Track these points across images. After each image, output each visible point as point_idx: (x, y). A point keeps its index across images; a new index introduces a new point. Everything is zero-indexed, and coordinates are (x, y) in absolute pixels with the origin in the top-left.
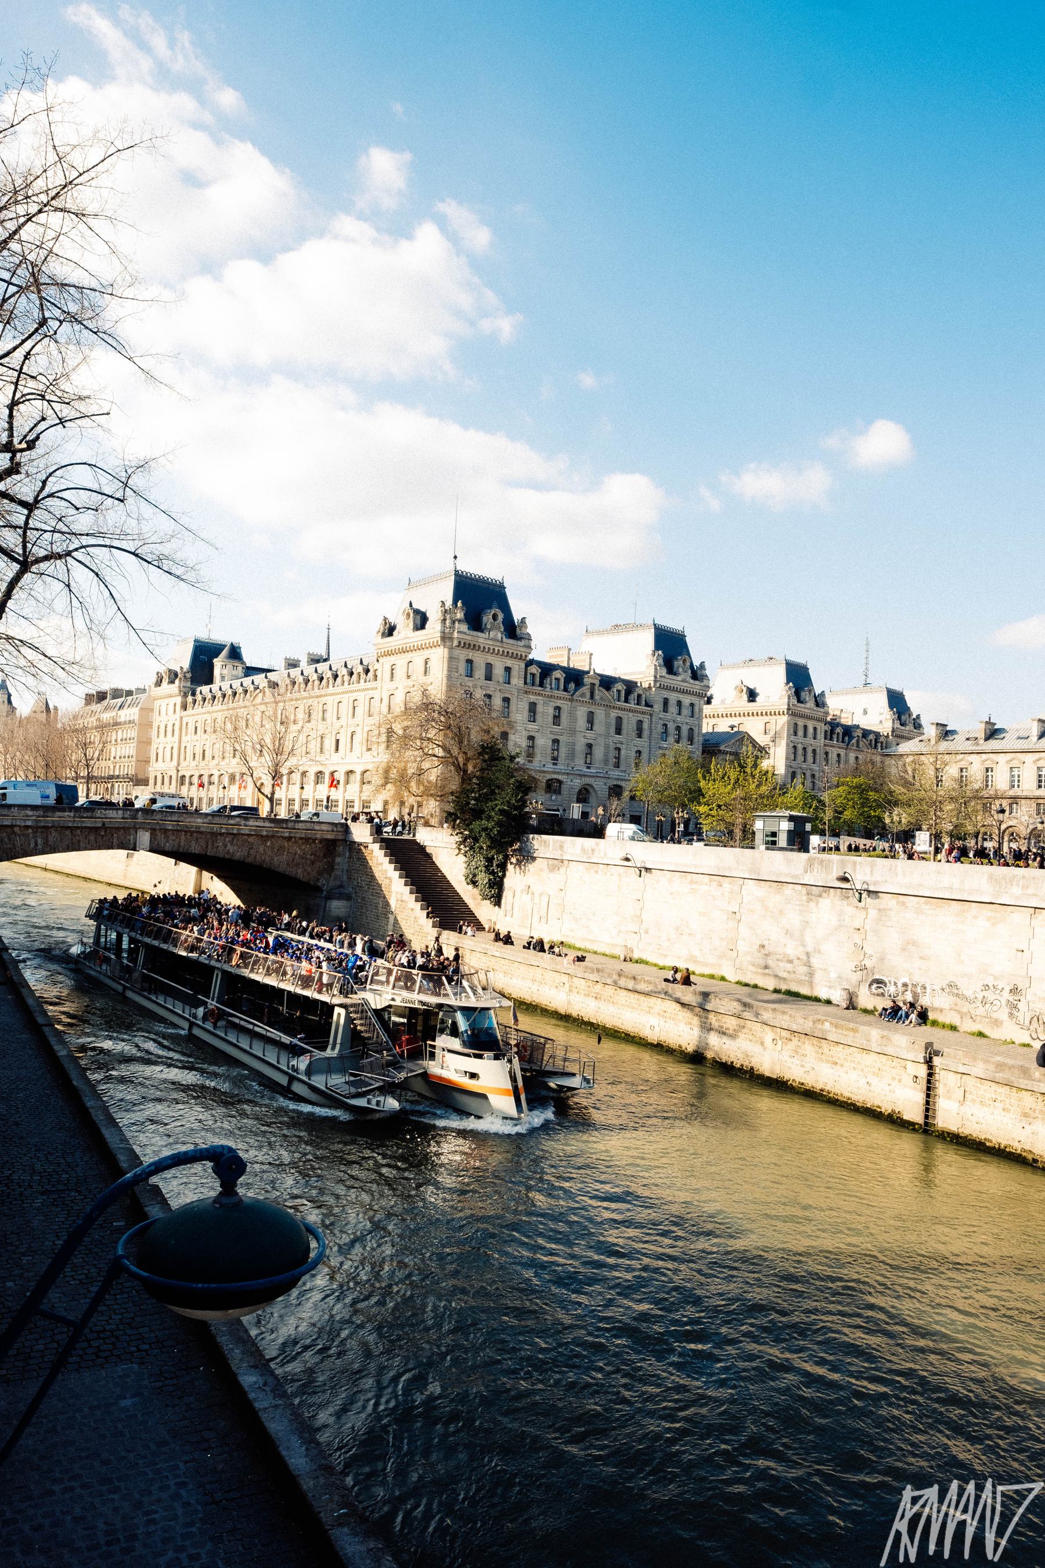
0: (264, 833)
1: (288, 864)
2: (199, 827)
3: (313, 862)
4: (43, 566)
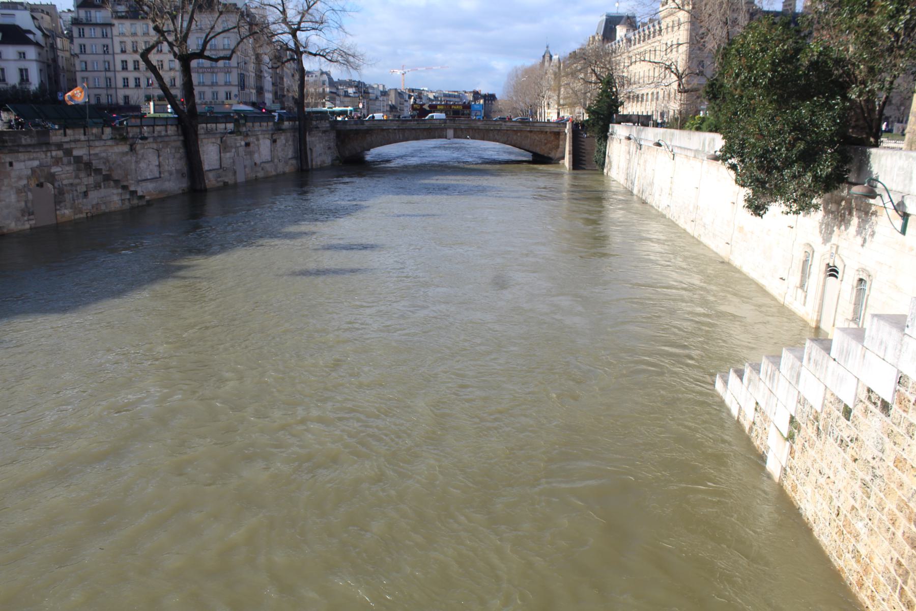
0: (515, 129)
3: (546, 144)
4: (351, 14)
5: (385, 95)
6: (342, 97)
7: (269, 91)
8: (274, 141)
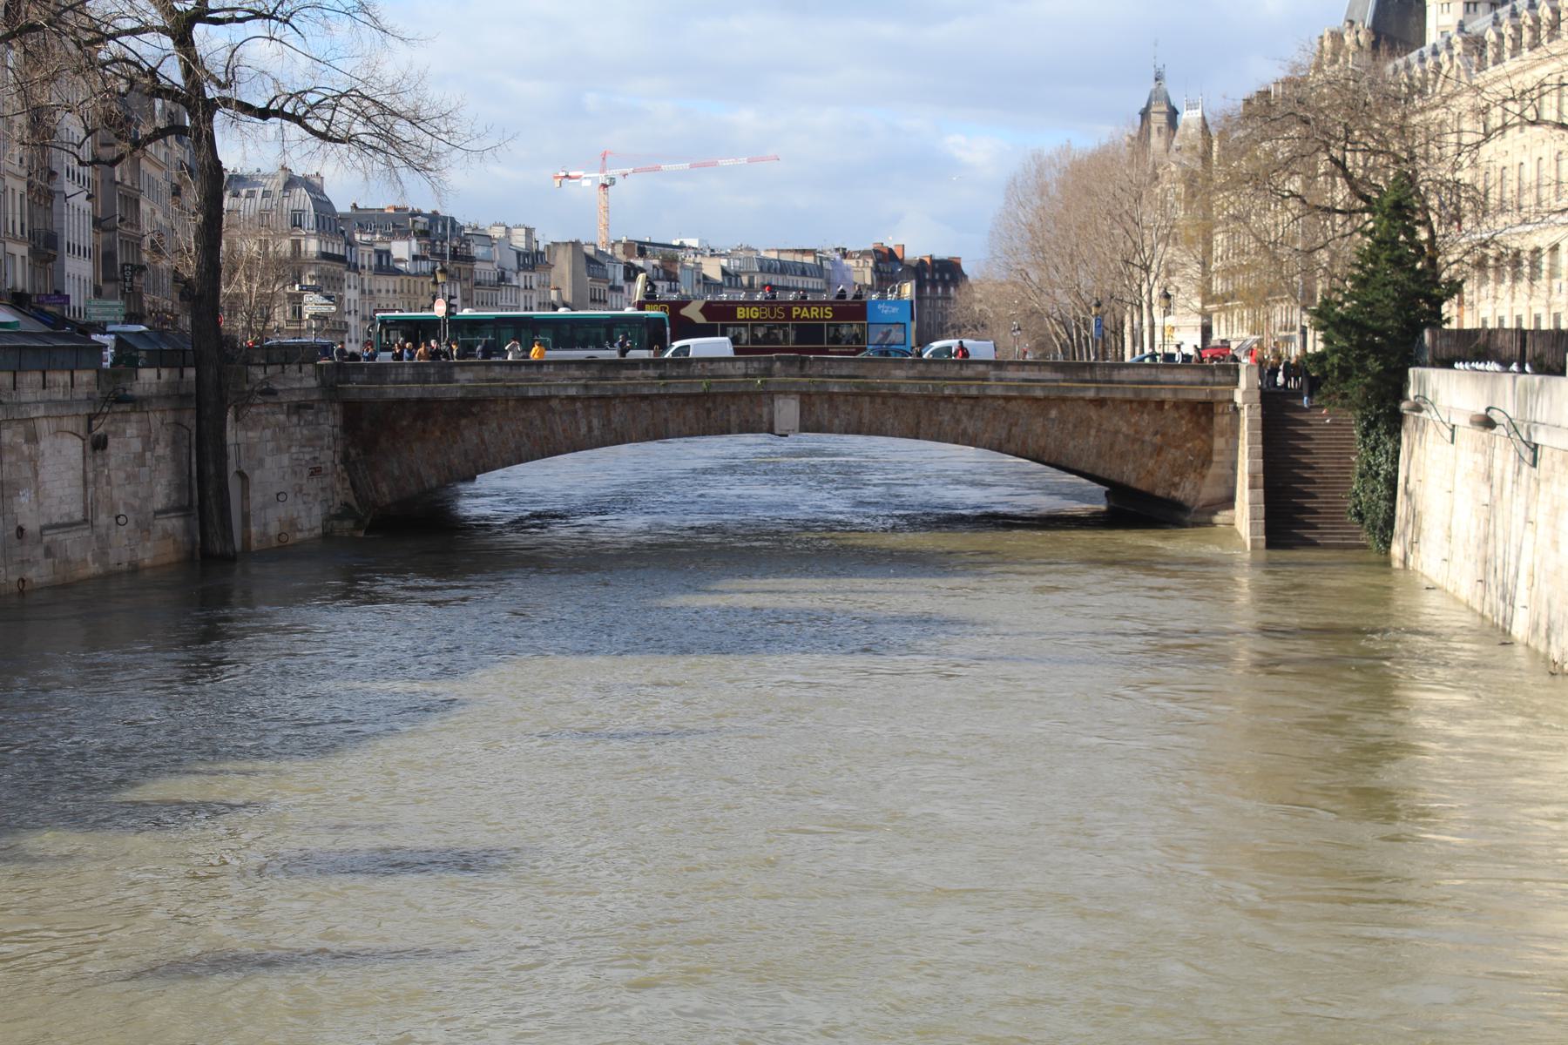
0: (1039, 393)
1: (1100, 455)
2: (896, 387)
3: (1159, 450)
5: (532, 268)
6: (367, 275)
7: (81, 252)
8: (100, 444)
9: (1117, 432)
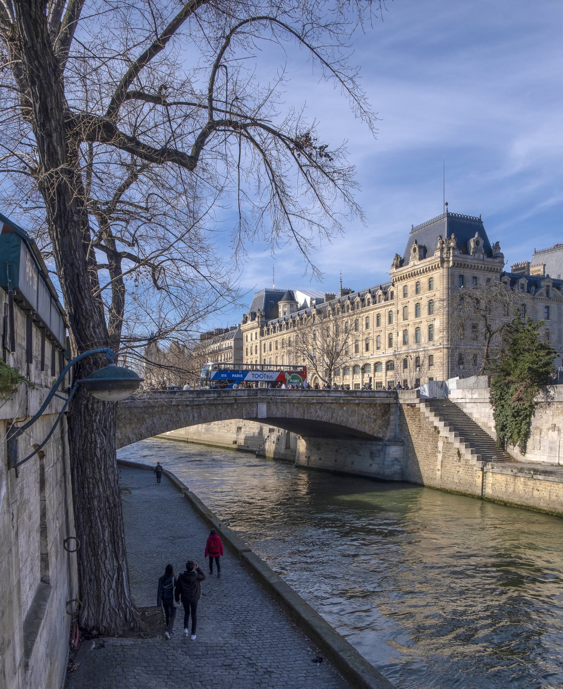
1: (358, 423)
3: (375, 420)
9: (363, 415)
